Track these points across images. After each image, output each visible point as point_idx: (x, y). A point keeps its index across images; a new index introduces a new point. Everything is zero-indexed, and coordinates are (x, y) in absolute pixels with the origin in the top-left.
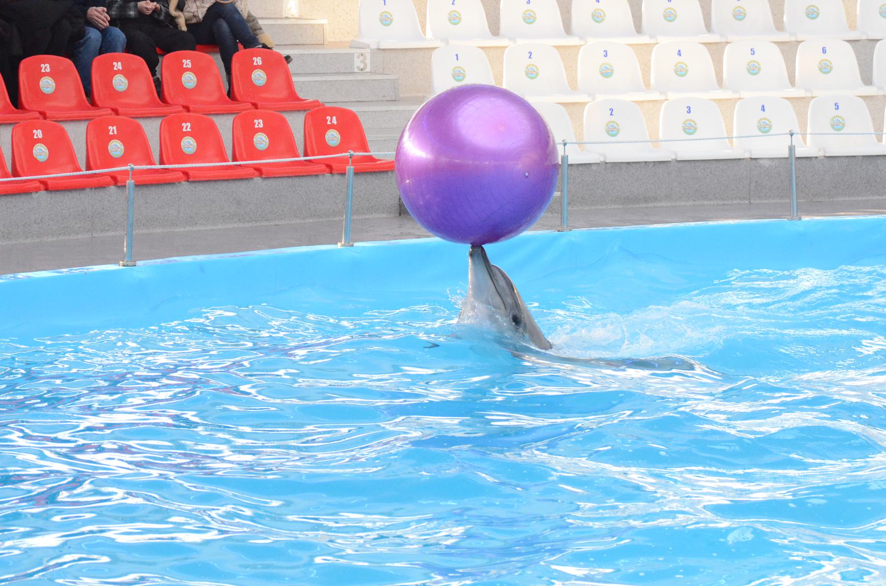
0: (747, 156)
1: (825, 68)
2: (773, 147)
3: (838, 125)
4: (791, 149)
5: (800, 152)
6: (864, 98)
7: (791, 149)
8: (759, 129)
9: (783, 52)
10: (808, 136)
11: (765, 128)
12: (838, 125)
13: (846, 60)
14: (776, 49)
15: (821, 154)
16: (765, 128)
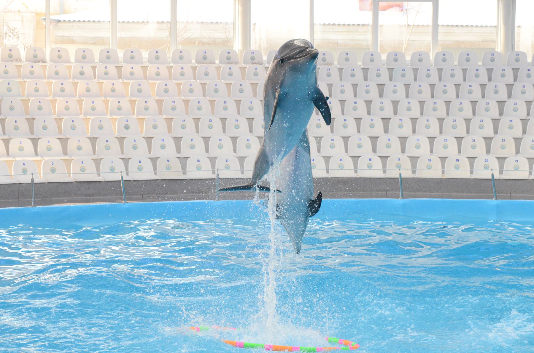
0: (17, 182)
1: (49, 149)
2: (26, 179)
3: (53, 171)
4: (32, 180)
5: (36, 181)
6: (64, 160)
7: (32, 180)
8: (23, 172)
9: (33, 143)
10: (71, 175)
11: (25, 172)
12: (53, 171)
13: (57, 146)
14: (30, 142)
15: (46, 182)
16: (25, 172)
